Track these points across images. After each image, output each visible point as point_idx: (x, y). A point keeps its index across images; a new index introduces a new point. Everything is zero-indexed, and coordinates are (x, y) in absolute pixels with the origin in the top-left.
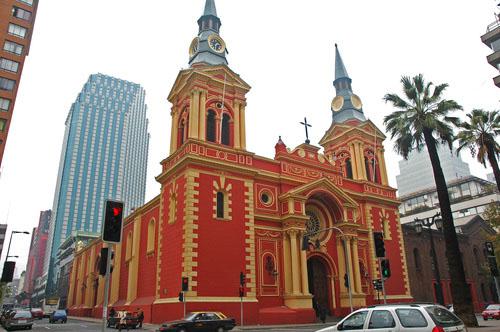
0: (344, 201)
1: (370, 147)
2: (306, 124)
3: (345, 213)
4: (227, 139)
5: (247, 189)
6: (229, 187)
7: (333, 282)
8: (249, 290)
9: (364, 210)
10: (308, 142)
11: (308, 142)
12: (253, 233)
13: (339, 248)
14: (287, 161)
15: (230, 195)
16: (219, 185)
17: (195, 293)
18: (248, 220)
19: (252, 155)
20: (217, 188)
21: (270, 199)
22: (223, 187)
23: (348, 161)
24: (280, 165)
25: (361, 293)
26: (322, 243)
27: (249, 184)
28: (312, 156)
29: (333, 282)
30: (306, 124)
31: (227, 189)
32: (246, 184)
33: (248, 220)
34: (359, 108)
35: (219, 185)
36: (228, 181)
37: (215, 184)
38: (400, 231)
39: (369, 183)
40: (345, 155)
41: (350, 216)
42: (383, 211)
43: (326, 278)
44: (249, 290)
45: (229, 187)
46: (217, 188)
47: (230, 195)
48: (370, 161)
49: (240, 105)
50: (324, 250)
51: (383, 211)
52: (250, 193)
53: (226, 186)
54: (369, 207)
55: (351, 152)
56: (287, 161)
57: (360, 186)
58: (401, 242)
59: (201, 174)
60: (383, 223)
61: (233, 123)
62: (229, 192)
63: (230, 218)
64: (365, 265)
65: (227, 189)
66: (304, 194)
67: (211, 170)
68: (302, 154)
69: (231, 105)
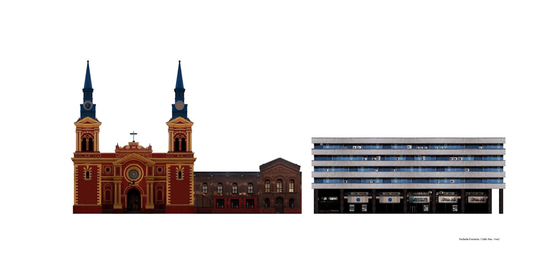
4: (91, 148)
6: (91, 168)
10: (134, 141)
11: (134, 141)
12: (101, 183)
15: (91, 171)
22: (88, 168)
27: (100, 166)
32: (98, 167)
35: (86, 168)
37: (84, 168)
47: (91, 171)
53: (89, 168)
59: (78, 166)
62: (91, 170)
63: (91, 179)
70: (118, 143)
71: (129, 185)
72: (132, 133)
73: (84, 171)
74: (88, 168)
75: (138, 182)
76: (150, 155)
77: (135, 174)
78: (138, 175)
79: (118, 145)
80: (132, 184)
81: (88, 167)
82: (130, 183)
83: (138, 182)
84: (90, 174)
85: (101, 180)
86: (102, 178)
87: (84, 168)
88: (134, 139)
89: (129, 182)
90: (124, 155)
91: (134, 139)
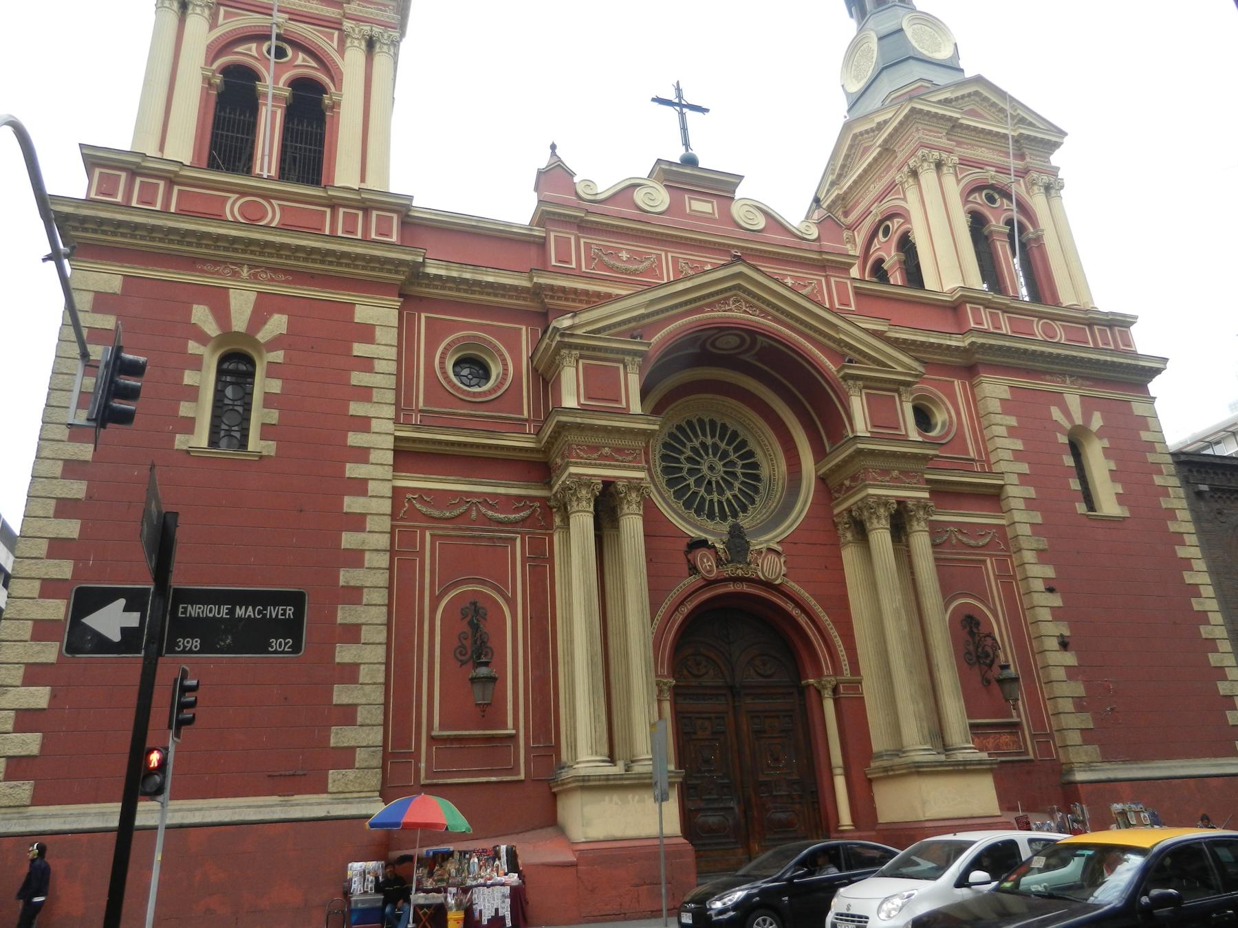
0: (844, 353)
1: (990, 175)
2: (680, 105)
3: (858, 406)
5: (367, 333)
6: (277, 324)
7: (829, 706)
8: (345, 758)
9: (974, 400)
12: (386, 506)
13: (850, 556)
14: (582, 226)
15: (278, 356)
16: (222, 312)
17: (24, 790)
18: (362, 455)
19: (402, 209)
20: (212, 329)
21: (495, 370)
23: (907, 246)
24: (542, 244)
25: (971, 754)
26: (758, 543)
28: (702, 206)
29: (829, 706)
30: (680, 105)
31: (263, 336)
33: (362, 455)
34: (944, 54)
36: (264, 307)
37: (201, 315)
38: (1169, 480)
39: (999, 299)
40: (895, 224)
41: (883, 420)
42: (1073, 401)
43: (803, 691)
44: (345, 758)
45: (277, 324)
46: (212, 329)
47: (278, 356)
48: (996, 224)
49: (371, 44)
50: (771, 568)
51: (1073, 401)
52: (383, 349)
54: (995, 389)
55: (912, 204)
56: (582, 226)
57: (954, 308)
58: (1183, 522)
60: (1076, 450)
61: (336, 105)
64: (999, 629)
65: (263, 336)
66: (637, 329)
67: (191, 263)
68: (658, 199)
69: (327, 44)
70: (553, 147)
71: (693, 569)
72: (672, 96)
73: (193, 347)
74: (239, 324)
75: (770, 539)
76: (841, 287)
77: (719, 466)
78: (757, 478)
79: (553, 153)
80: (719, 561)
81: (242, 303)
82: (703, 543)
83: (770, 539)
84: (263, 385)
85: (388, 472)
86: (397, 439)
87: (201, 315)
88: (686, 144)
89: (695, 533)
90: (624, 255)
91: (686, 144)
